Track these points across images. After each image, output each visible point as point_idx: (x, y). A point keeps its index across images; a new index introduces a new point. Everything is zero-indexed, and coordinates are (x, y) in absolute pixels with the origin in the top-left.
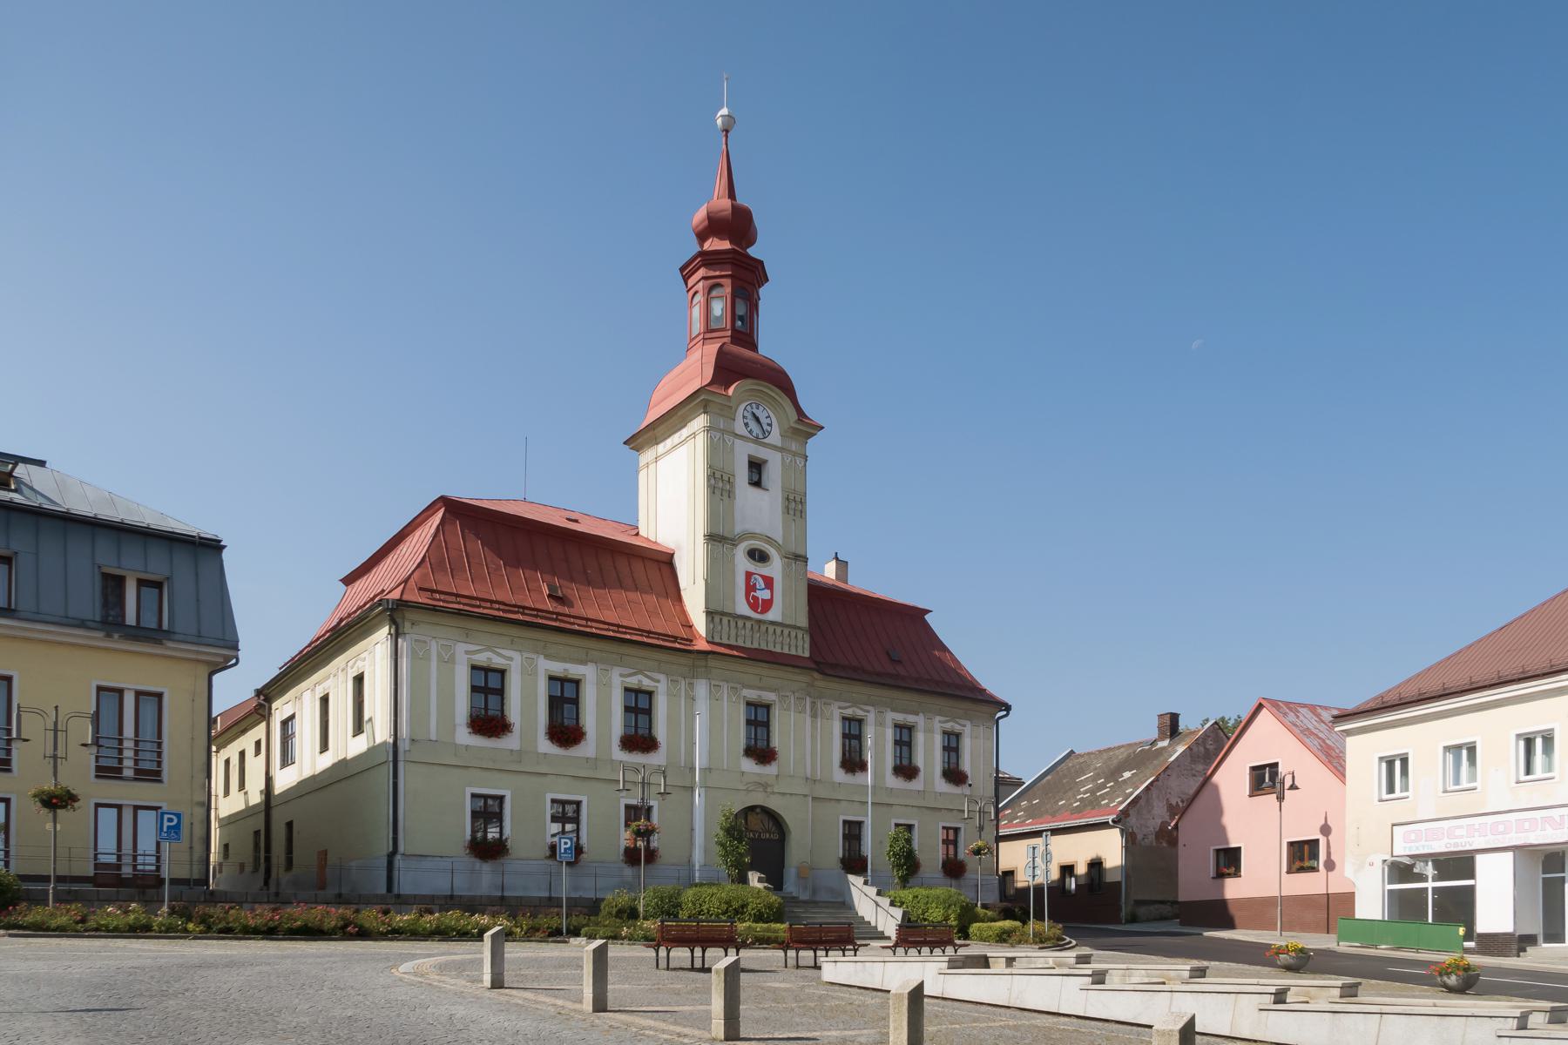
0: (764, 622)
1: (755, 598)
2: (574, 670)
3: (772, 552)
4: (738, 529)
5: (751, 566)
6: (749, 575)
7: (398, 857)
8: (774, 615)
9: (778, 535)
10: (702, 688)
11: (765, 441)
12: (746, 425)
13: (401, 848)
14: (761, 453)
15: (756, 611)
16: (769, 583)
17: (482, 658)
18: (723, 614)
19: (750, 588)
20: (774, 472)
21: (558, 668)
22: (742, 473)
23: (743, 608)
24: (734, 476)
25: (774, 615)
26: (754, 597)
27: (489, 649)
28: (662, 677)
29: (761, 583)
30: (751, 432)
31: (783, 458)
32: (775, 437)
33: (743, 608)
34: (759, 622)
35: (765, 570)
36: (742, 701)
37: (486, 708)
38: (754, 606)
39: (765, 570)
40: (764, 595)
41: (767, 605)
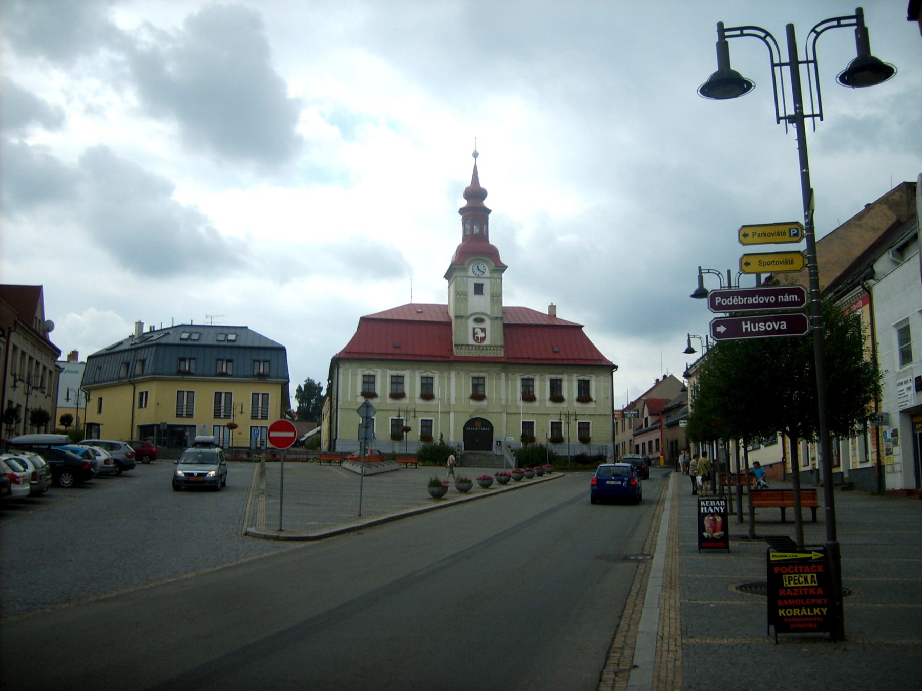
0: (481, 346)
1: (478, 338)
2: (400, 373)
3: (485, 318)
4: (469, 312)
5: (476, 325)
6: (474, 329)
7: (337, 440)
8: (487, 342)
9: (489, 313)
10: (453, 375)
11: (483, 276)
12: (474, 272)
13: (338, 437)
14: (480, 281)
15: (478, 342)
16: (483, 330)
17: (367, 372)
18: (462, 345)
19: (474, 334)
20: (487, 289)
21: (394, 373)
22: (471, 289)
23: (471, 341)
24: (468, 292)
25: (487, 342)
26: (477, 337)
27: (369, 369)
28: (436, 372)
29: (479, 331)
30: (476, 274)
31: (491, 281)
32: (487, 274)
33: (471, 341)
34: (479, 346)
35: (482, 326)
36: (470, 377)
37: (369, 389)
38: (476, 339)
39: (482, 326)
40: (481, 335)
41: (483, 339)
